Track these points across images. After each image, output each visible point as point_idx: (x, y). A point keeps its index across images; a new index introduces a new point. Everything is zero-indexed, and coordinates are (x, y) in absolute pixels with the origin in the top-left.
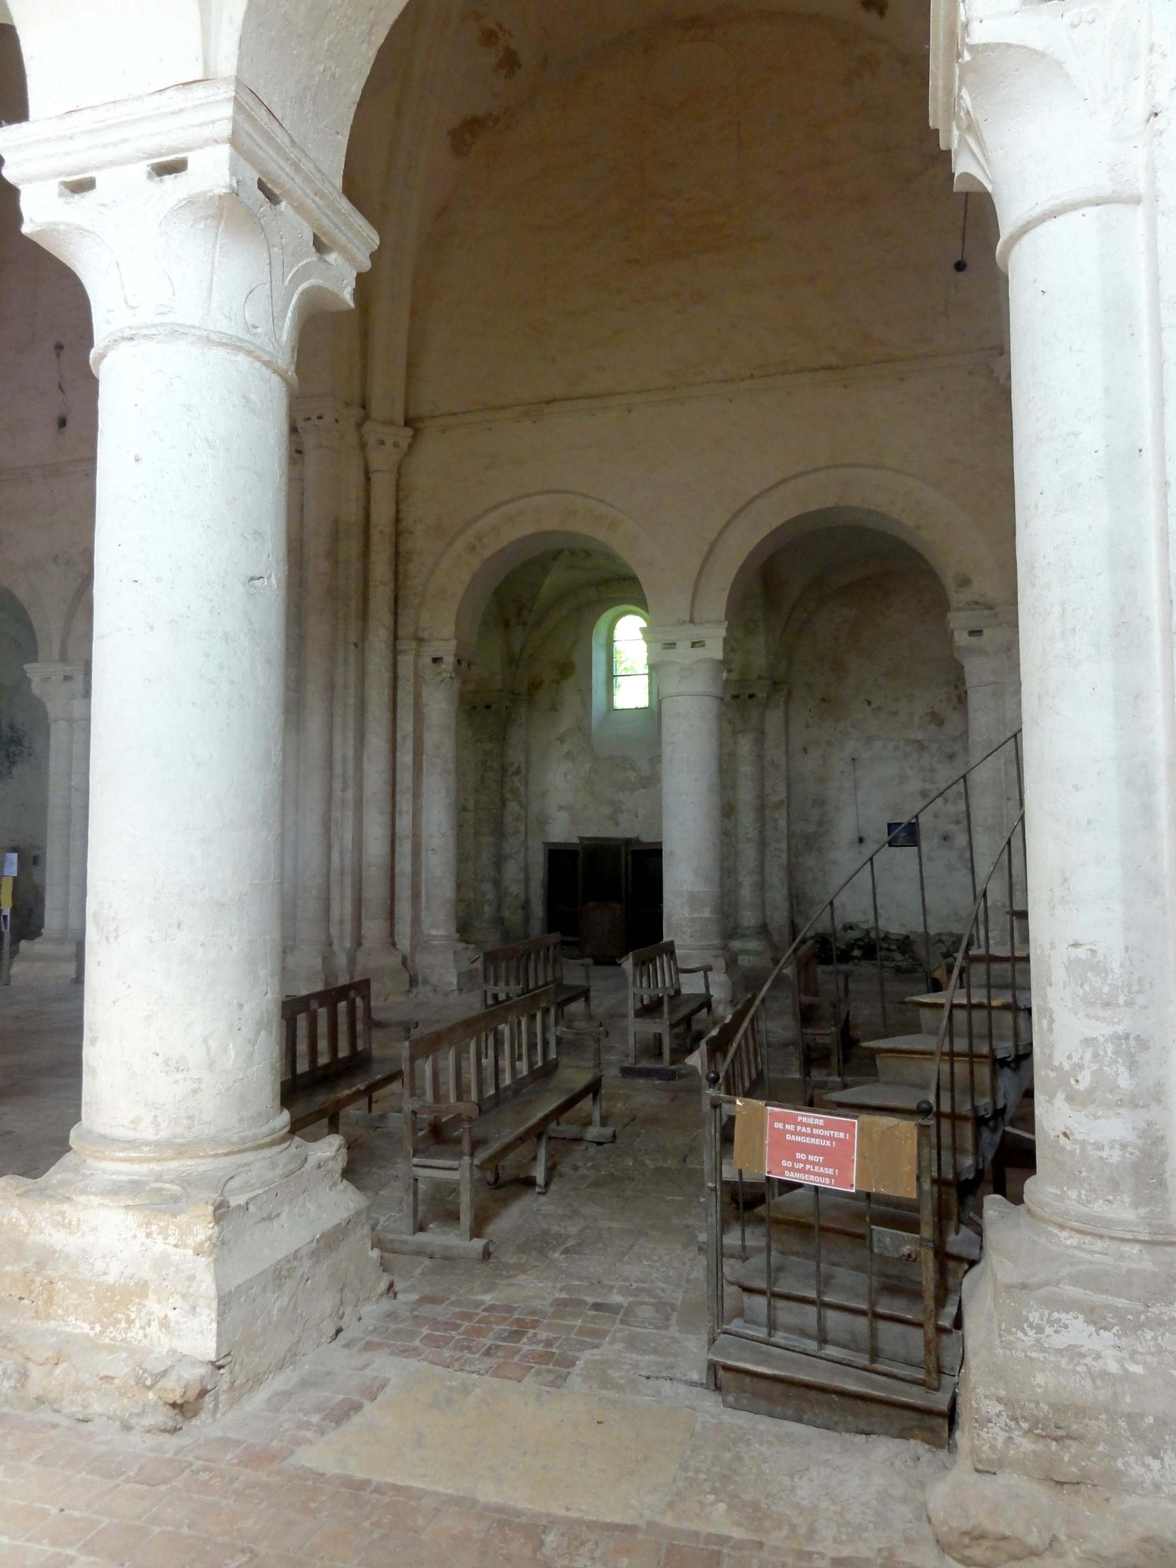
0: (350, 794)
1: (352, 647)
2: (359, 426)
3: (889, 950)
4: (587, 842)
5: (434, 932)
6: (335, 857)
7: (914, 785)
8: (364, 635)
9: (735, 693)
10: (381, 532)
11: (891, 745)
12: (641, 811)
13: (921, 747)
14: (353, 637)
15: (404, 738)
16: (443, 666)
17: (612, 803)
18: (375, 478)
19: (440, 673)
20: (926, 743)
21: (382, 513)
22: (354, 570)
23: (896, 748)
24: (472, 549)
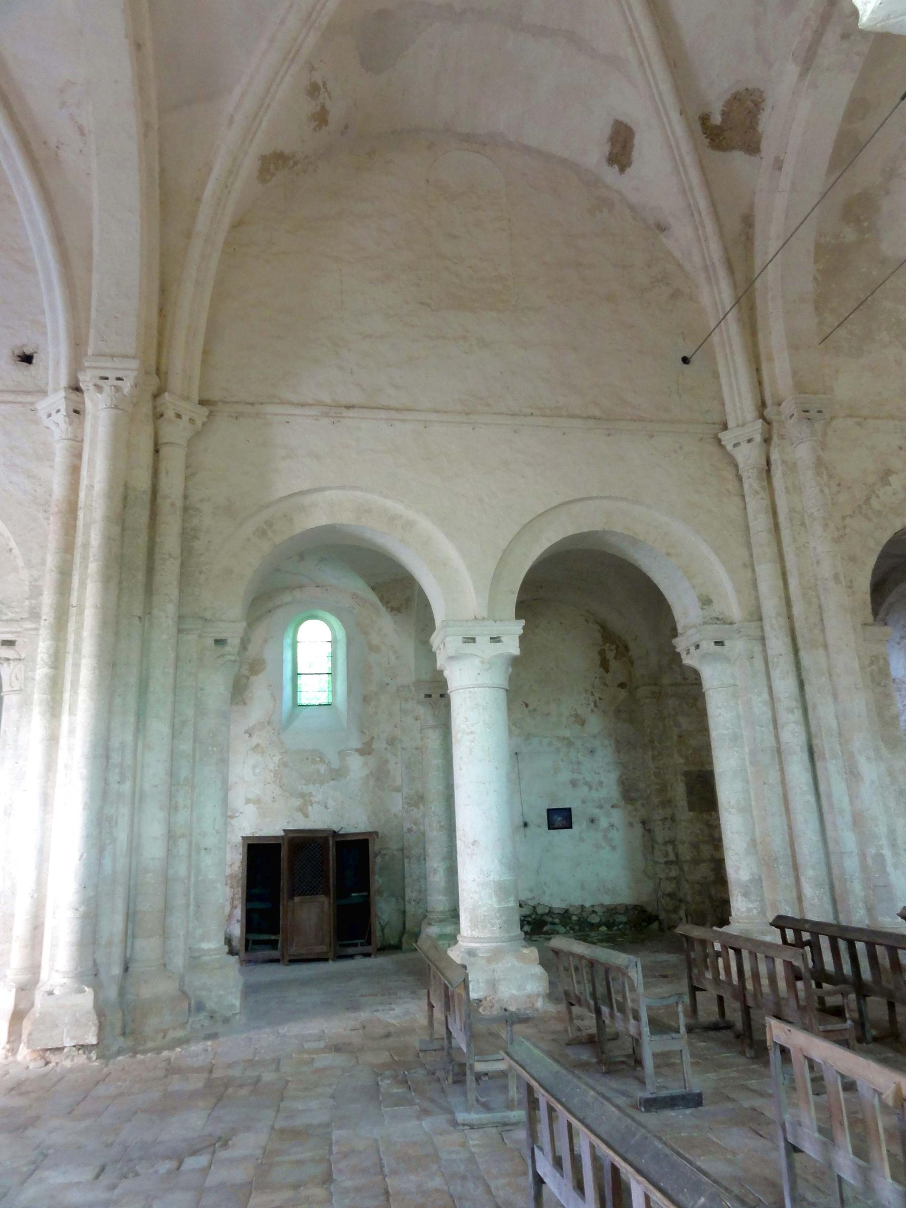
0: (127, 787)
1: (136, 621)
2: (156, 396)
3: (553, 924)
4: (291, 835)
5: (205, 946)
6: (107, 862)
7: (565, 776)
8: (148, 609)
9: (428, 693)
10: (173, 505)
11: (545, 741)
12: (331, 803)
13: (569, 743)
14: (138, 610)
15: (184, 723)
16: (228, 649)
17: (302, 795)
18: (164, 451)
19: (223, 656)
20: (572, 739)
21: (173, 485)
22: (142, 540)
23: (550, 744)
24: (262, 533)
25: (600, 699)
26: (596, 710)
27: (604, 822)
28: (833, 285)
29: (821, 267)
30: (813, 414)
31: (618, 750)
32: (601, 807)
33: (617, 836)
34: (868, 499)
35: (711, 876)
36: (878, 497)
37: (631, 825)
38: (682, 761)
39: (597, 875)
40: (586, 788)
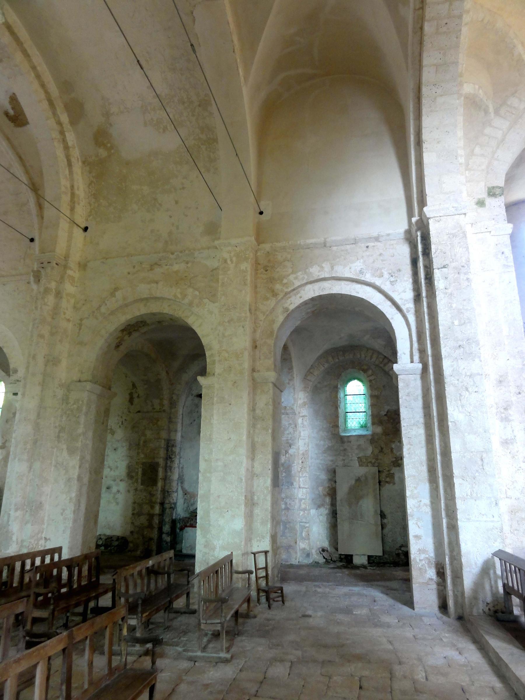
25: (125, 420)
26: (122, 426)
27: (114, 489)
28: (103, 183)
29: (94, 175)
30: (45, 264)
31: (130, 449)
32: (114, 480)
33: (121, 497)
34: (100, 306)
35: (146, 524)
36: (106, 305)
37: (129, 491)
38: (142, 456)
39: (106, 518)
40: (109, 470)
